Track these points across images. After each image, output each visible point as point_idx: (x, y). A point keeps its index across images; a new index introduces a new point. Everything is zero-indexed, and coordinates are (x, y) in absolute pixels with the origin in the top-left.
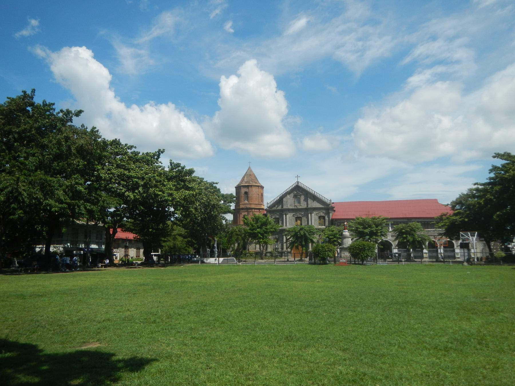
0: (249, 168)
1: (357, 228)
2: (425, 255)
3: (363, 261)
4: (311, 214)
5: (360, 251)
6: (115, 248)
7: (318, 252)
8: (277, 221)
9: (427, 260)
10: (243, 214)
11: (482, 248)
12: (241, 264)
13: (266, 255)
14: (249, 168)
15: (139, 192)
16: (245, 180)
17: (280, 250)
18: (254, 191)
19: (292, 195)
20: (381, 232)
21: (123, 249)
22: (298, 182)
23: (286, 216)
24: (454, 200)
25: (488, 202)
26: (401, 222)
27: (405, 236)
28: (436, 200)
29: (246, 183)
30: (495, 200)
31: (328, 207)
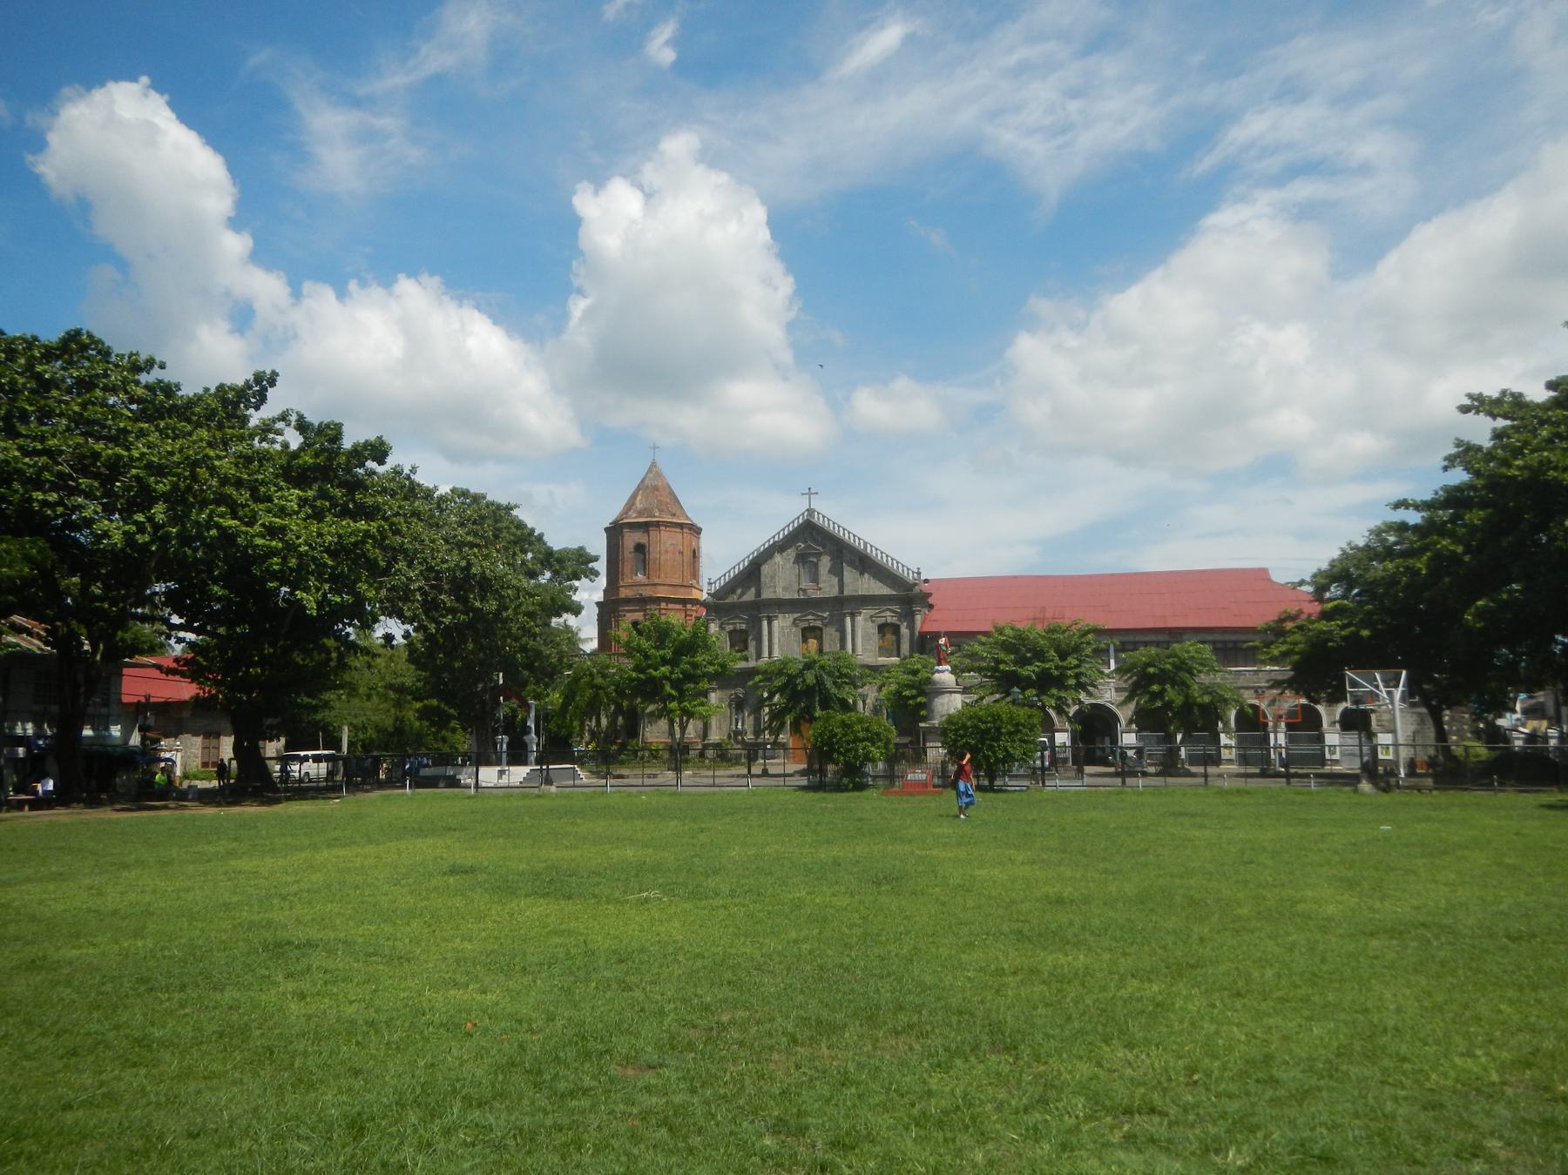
0: (654, 464)
1: (998, 661)
2: (1225, 754)
3: (992, 776)
4: (853, 615)
5: (982, 741)
6: (167, 737)
7: (831, 745)
8: (740, 640)
9: (1234, 768)
10: (631, 617)
11: (1413, 728)
12: (553, 789)
13: (702, 755)
14: (654, 464)
15: (150, 519)
16: (638, 505)
17: (749, 737)
18: (666, 544)
19: (791, 553)
20: (1077, 676)
21: (199, 740)
22: (810, 511)
23: (770, 624)
24: (1325, 566)
25: (1443, 563)
26: (1146, 644)
27: (1155, 688)
28: (1264, 571)
29: (640, 514)
30: (1467, 558)
31: (909, 596)
